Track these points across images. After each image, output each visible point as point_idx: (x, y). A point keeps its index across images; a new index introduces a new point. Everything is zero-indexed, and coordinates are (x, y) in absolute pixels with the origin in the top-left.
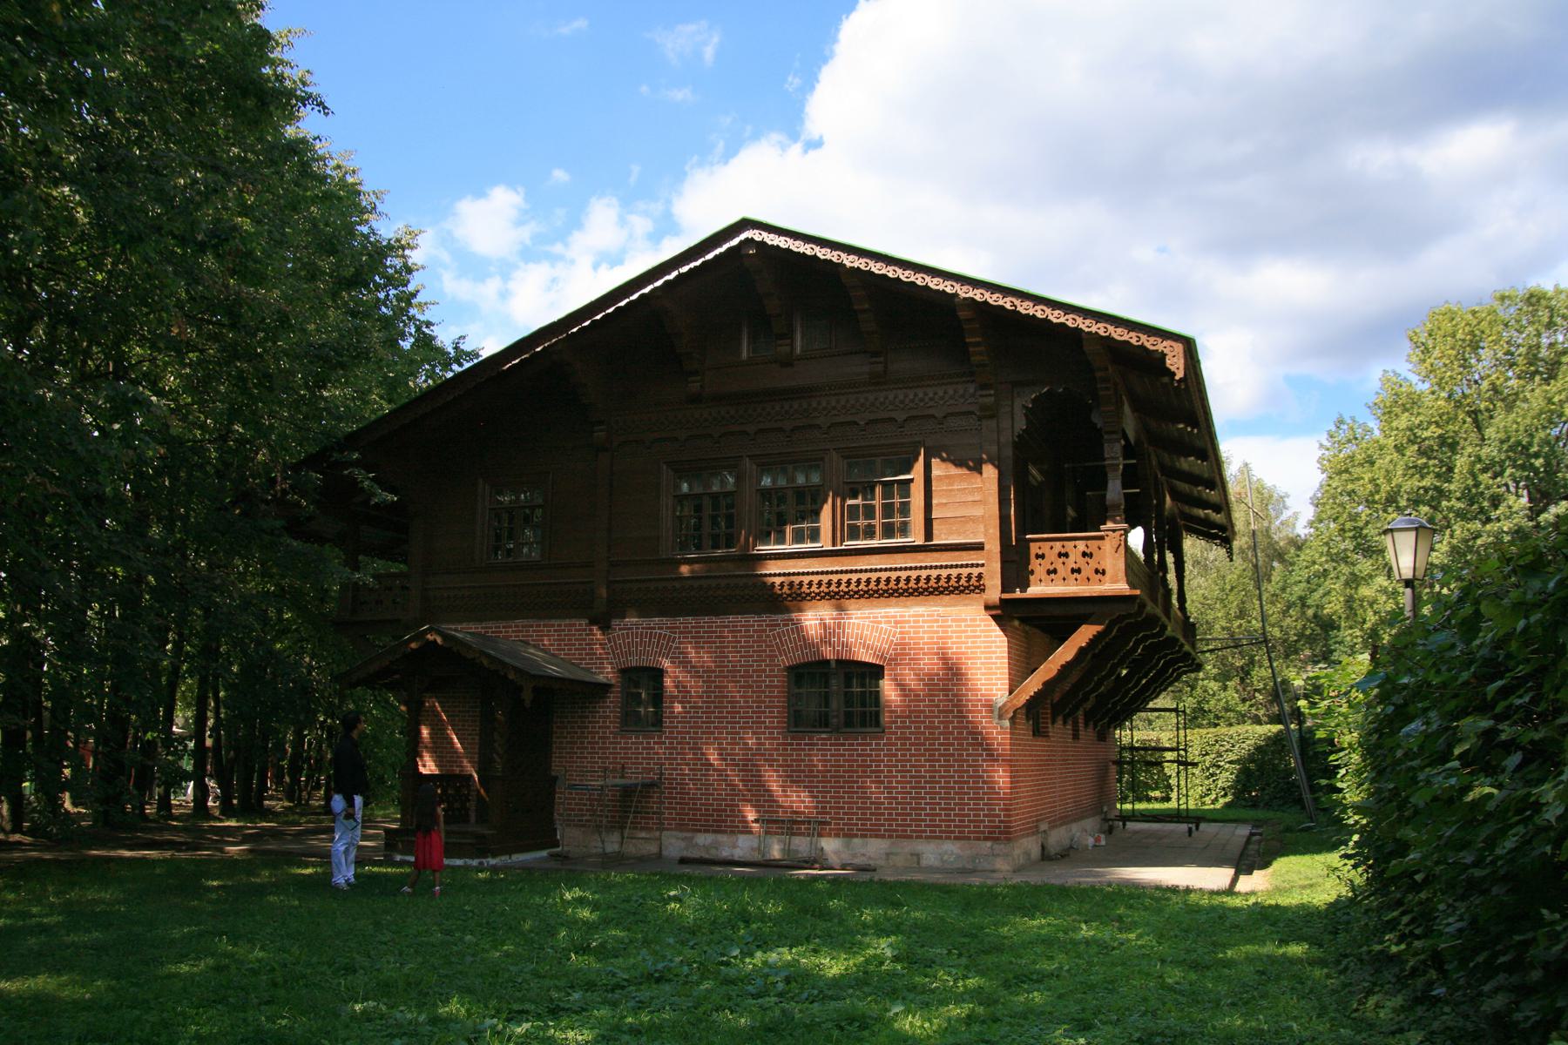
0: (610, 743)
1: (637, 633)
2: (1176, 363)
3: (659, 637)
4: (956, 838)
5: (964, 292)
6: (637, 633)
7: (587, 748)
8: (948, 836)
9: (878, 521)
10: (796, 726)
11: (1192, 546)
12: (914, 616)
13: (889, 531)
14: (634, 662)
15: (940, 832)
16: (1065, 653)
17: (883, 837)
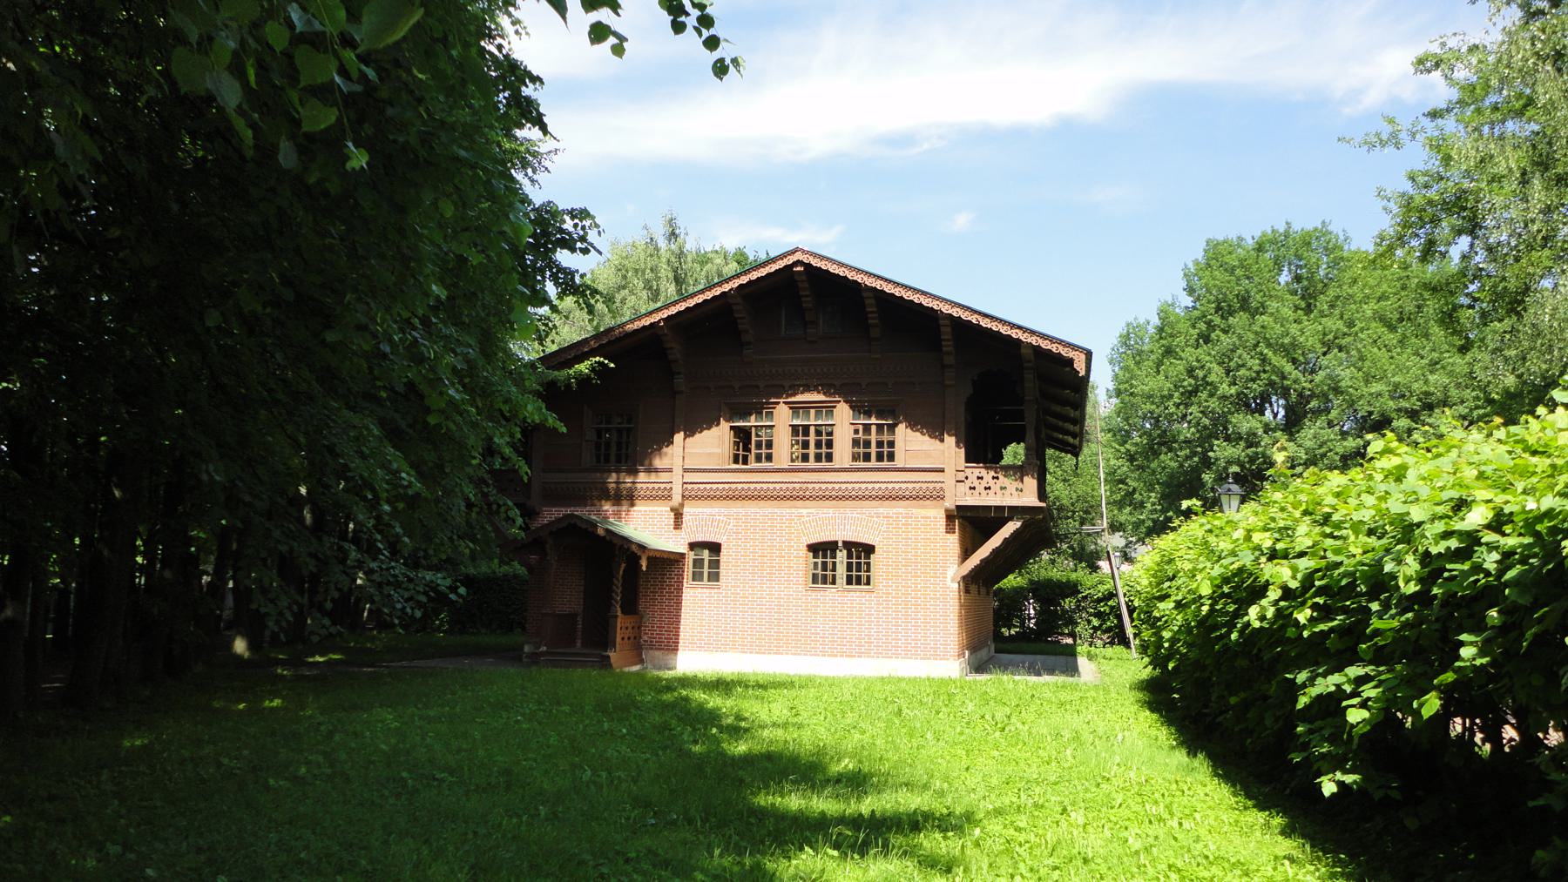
2: (1080, 366)
5: (946, 309)
9: (873, 450)
10: (813, 583)
13: (880, 458)
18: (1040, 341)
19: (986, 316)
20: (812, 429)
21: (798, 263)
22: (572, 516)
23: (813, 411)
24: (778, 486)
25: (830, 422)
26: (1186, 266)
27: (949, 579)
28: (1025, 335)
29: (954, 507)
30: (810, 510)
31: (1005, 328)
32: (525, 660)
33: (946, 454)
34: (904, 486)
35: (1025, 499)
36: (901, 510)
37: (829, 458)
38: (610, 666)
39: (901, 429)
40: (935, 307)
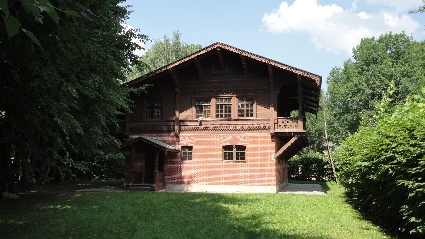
0: (179, 164)
1: (186, 138)
2: (318, 82)
3: (191, 139)
4: (263, 186)
5: (270, 63)
6: (186, 138)
7: (173, 165)
9: (245, 113)
12: (253, 135)
13: (247, 116)
15: (259, 184)
17: (246, 185)
18: (304, 74)
19: (284, 65)
20: (224, 106)
21: (218, 47)
22: (140, 137)
23: (224, 100)
24: (212, 126)
25: (230, 103)
26: (354, 48)
27: (272, 158)
28: (298, 72)
29: (274, 133)
30: (223, 134)
31: (291, 69)
32: (124, 188)
33: (271, 114)
34: (256, 125)
35: (299, 129)
36: (255, 134)
37: (230, 116)
38: (154, 190)
39: (255, 105)
40: (266, 62)
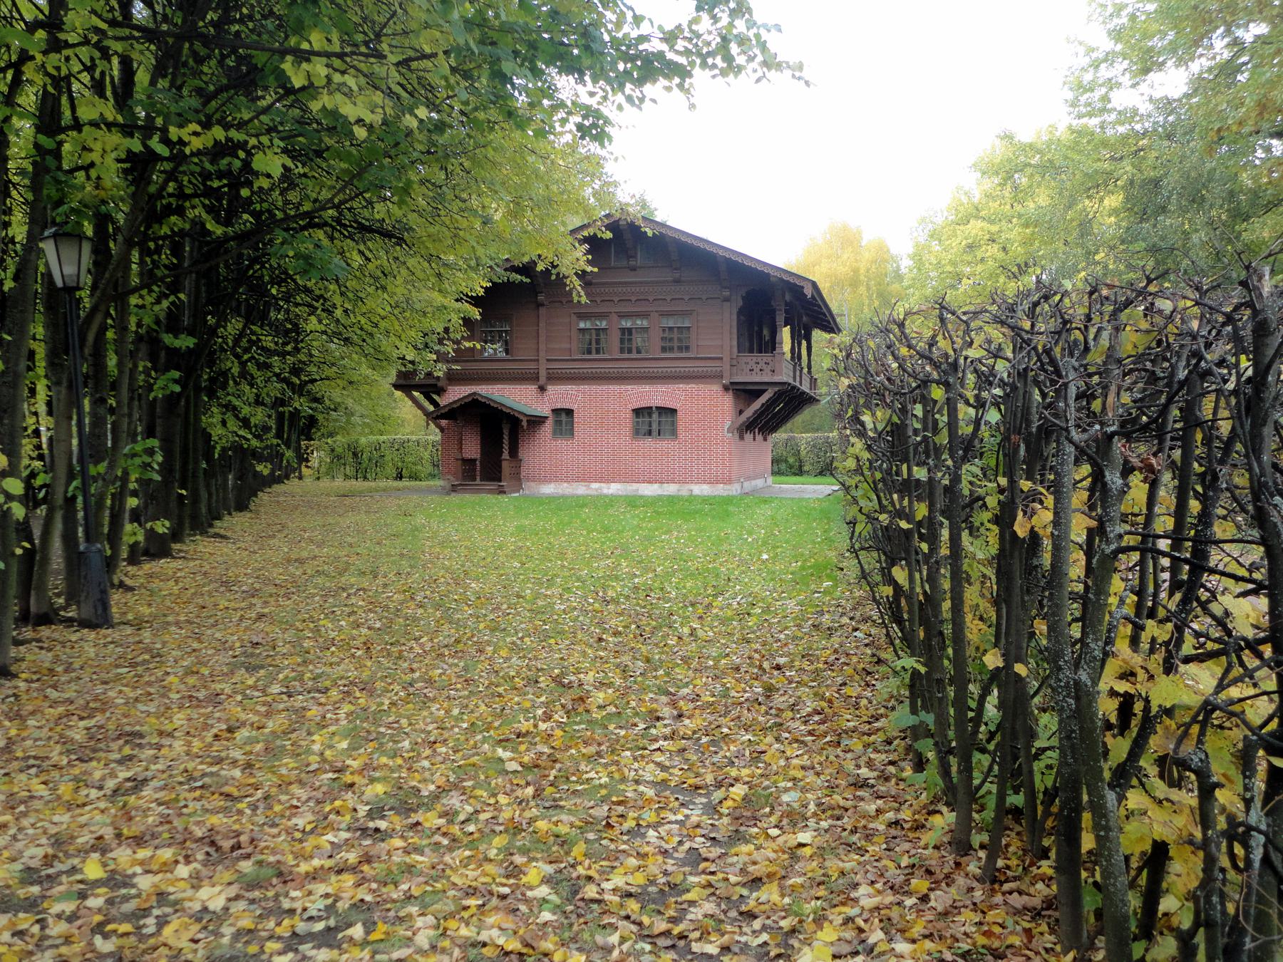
8: (704, 482)
11: (817, 335)
13: (680, 349)
14: (559, 406)
16: (757, 404)
22: (474, 394)
